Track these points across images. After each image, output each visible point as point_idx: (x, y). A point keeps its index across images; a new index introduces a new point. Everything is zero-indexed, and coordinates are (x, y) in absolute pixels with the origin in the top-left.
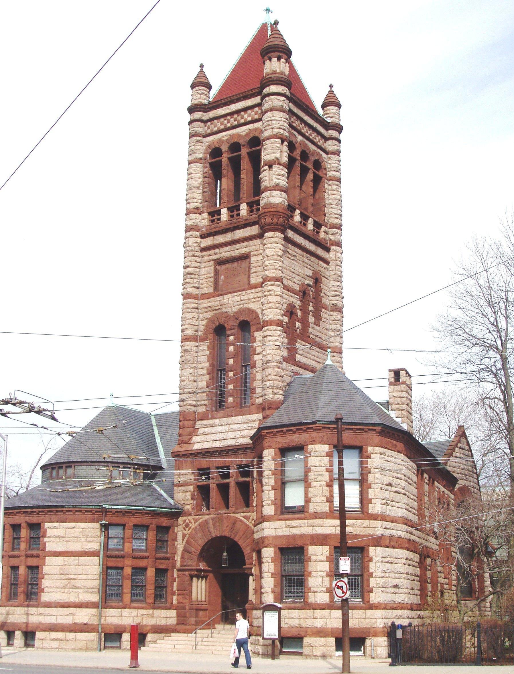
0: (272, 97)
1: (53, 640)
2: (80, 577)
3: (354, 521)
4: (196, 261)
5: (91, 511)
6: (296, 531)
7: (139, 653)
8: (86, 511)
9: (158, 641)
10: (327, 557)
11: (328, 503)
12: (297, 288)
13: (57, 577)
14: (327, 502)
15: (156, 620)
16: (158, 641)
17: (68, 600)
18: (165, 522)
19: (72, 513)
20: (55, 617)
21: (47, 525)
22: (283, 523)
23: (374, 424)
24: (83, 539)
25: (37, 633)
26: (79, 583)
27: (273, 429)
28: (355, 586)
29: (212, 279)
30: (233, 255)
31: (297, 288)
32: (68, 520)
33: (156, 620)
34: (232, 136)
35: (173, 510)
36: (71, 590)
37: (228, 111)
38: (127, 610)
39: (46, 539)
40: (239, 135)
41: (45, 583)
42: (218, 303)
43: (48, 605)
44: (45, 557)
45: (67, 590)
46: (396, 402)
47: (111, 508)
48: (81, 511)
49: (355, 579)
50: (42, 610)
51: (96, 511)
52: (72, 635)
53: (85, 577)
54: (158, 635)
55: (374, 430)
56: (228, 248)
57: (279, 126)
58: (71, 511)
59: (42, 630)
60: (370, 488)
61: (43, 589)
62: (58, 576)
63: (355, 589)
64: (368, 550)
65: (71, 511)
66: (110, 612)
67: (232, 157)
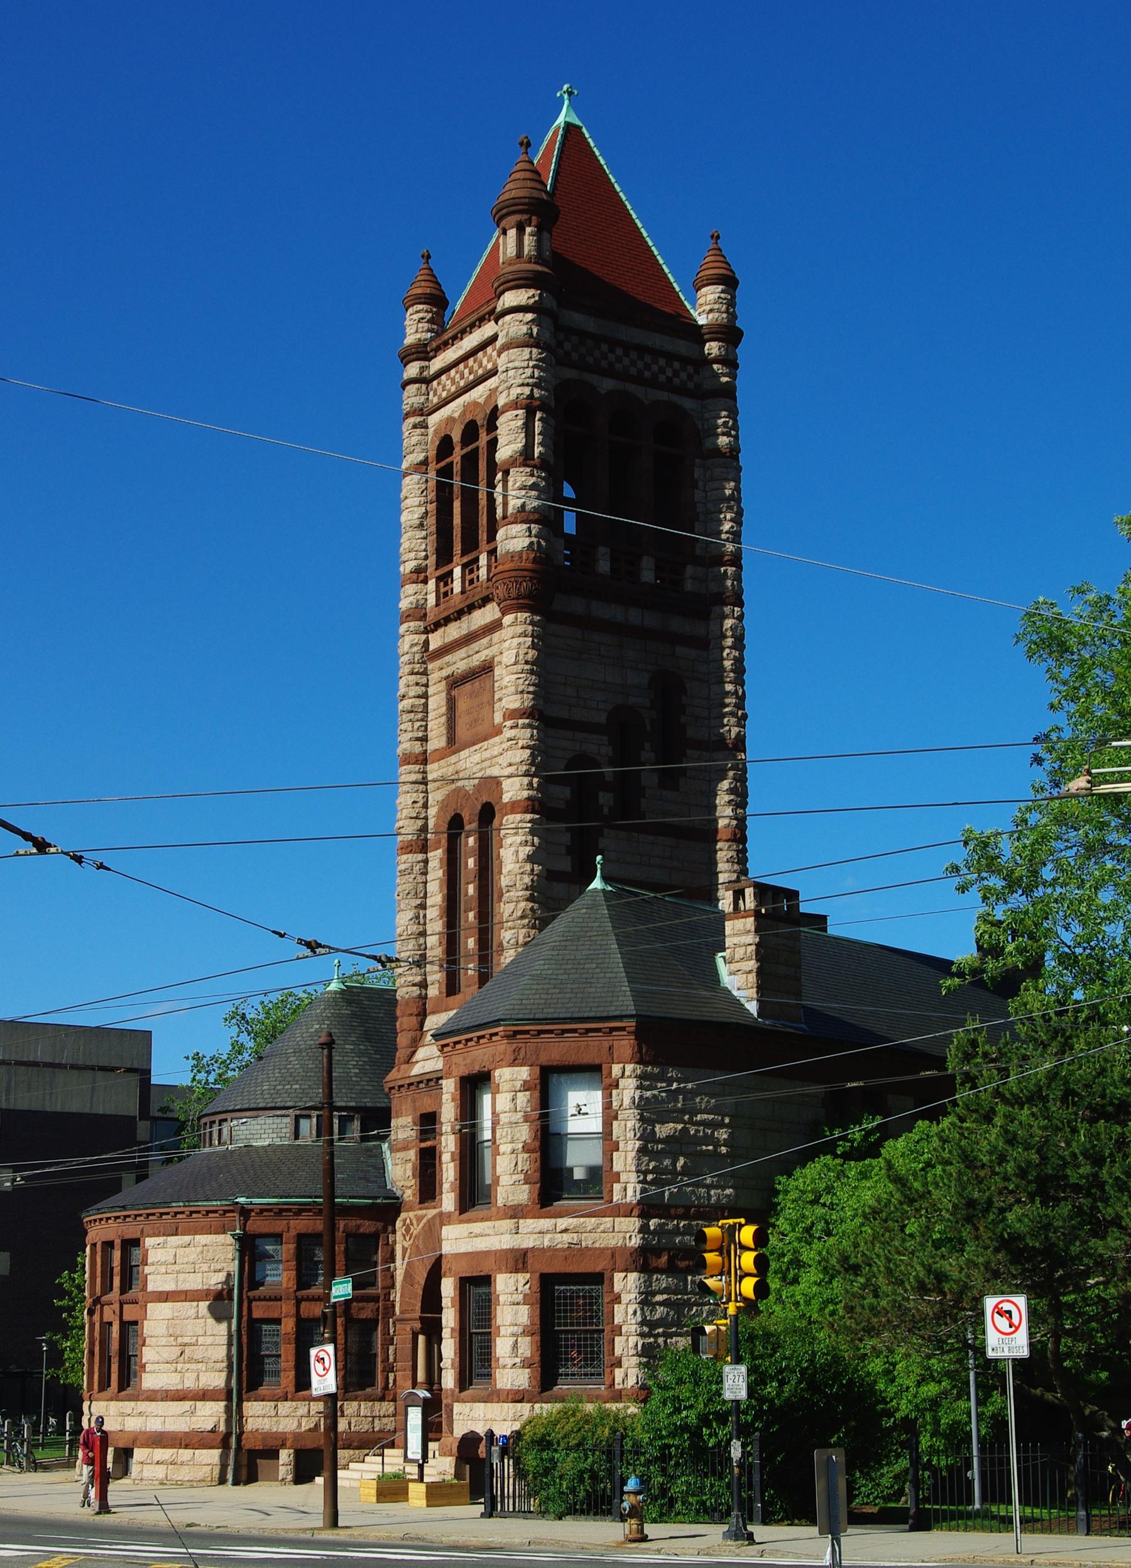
0: (508, 318)
1: (158, 1463)
2: (201, 1340)
3: (582, 1220)
4: (417, 684)
5: (216, 1212)
6: (481, 1245)
7: (110, 1487)
8: (208, 1212)
9: (352, 1465)
10: (525, 1295)
11: (527, 1186)
12: (602, 718)
13: (163, 1341)
14: (526, 1183)
15: (350, 1424)
16: (352, 1465)
17: (180, 1387)
18: (367, 1226)
19: (184, 1216)
20: (159, 1420)
21: (149, 1242)
22: (545, 1223)
23: (620, 1018)
24: (205, 1267)
25: (136, 1450)
26: (199, 1353)
27: (462, 1034)
28: (592, 1352)
29: (444, 719)
30: (471, 665)
31: (602, 718)
32: (180, 1230)
33: (350, 1424)
34: (466, 408)
35: (379, 1201)
36: (187, 1366)
37: (460, 353)
38: (288, 1404)
39: (147, 1270)
40: (475, 404)
41: (148, 1354)
42: (451, 770)
43: (153, 1396)
44: (146, 1302)
45: (179, 1366)
46: (737, 957)
47: (251, 1203)
48: (199, 1212)
49: (592, 1339)
50: (143, 1406)
51: (225, 1212)
52: (185, 1454)
53: (209, 1340)
54: (351, 1452)
55: (623, 1029)
56: (462, 653)
57: (521, 381)
58: (183, 1213)
59: (142, 1446)
60: (617, 1150)
61: (144, 1366)
62: (165, 1339)
63: (592, 1359)
64: (612, 1279)
65: (183, 1213)
66: (252, 1408)
67: (467, 453)
